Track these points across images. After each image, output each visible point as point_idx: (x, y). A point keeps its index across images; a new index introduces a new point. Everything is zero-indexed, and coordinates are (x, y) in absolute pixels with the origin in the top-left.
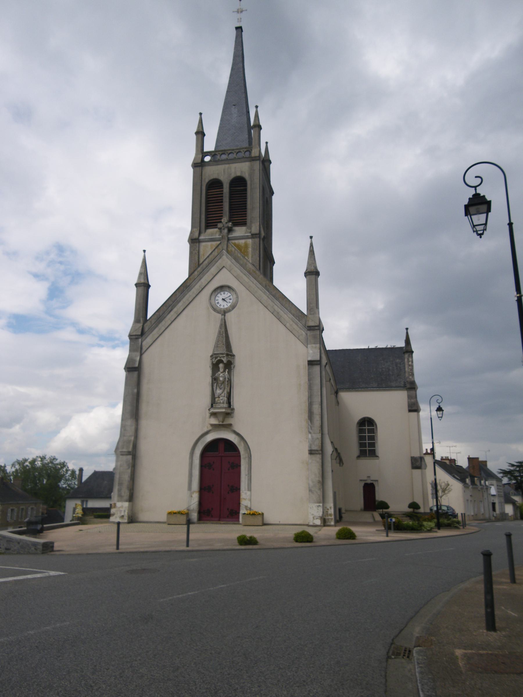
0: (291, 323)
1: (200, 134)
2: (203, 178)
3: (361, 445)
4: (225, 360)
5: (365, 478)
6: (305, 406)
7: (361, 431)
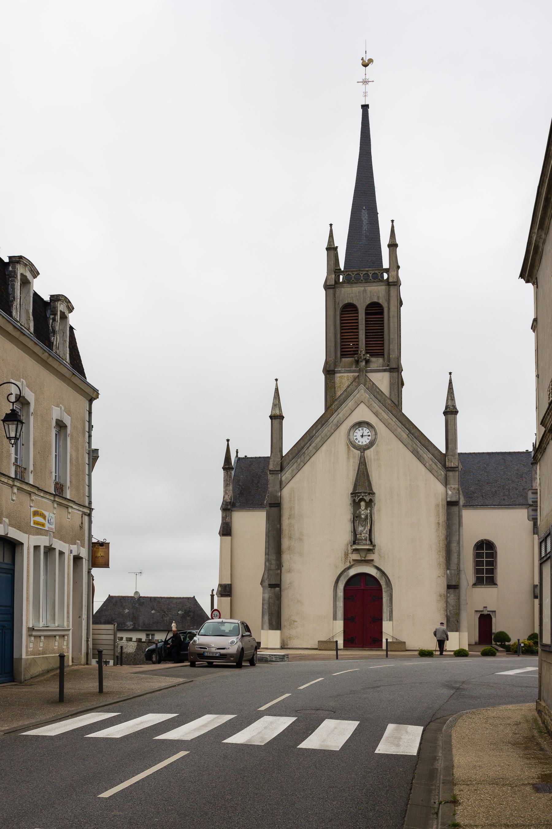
0: (431, 462)
1: (332, 249)
2: (337, 301)
3: (478, 571)
4: (367, 499)
5: (481, 609)
6: (442, 545)
7: (478, 555)
